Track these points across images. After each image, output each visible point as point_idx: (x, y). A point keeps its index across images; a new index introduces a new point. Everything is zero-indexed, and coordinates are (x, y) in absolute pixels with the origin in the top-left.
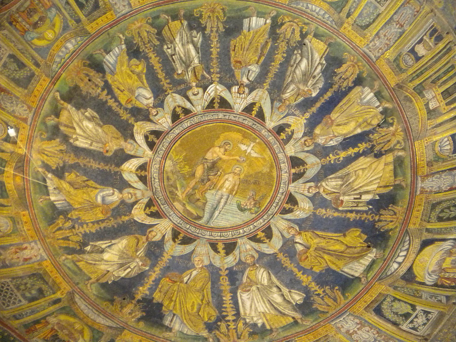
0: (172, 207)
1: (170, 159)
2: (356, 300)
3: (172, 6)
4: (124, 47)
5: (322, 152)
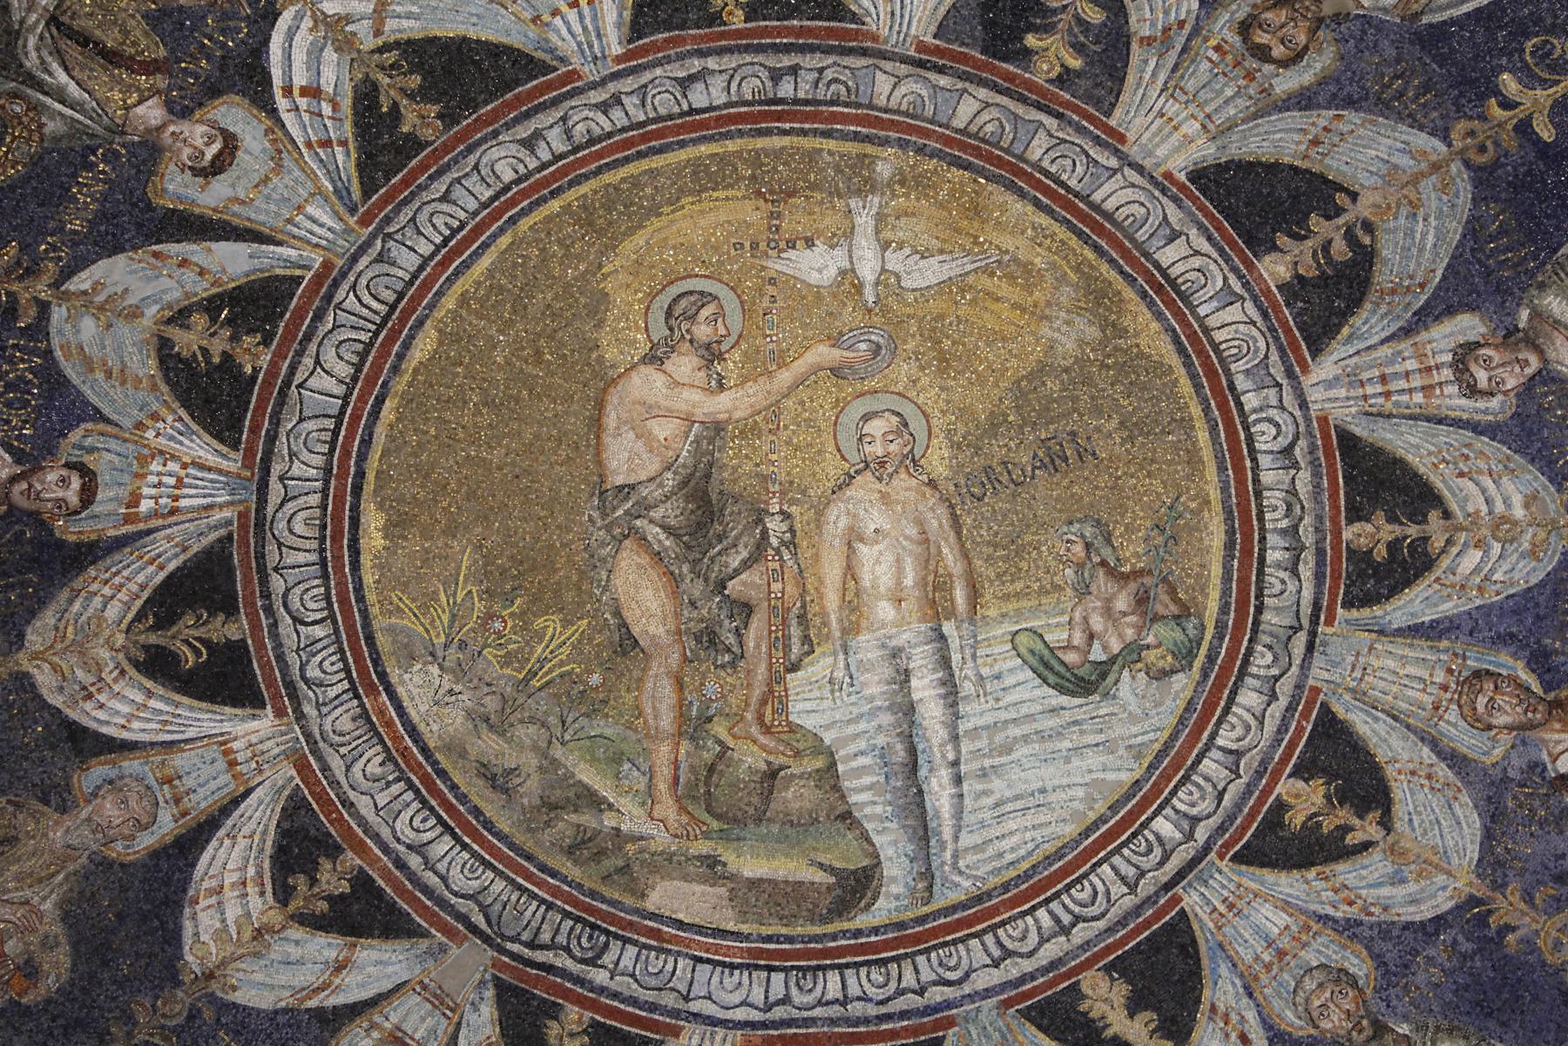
0: (659, 934)
1: (409, 658)
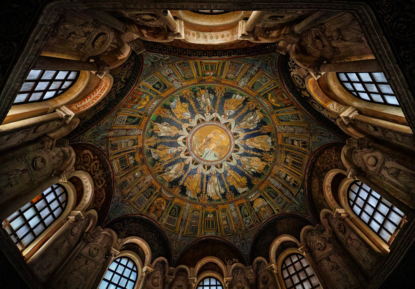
0: (193, 152)
3: (202, 85)
5: (246, 148)
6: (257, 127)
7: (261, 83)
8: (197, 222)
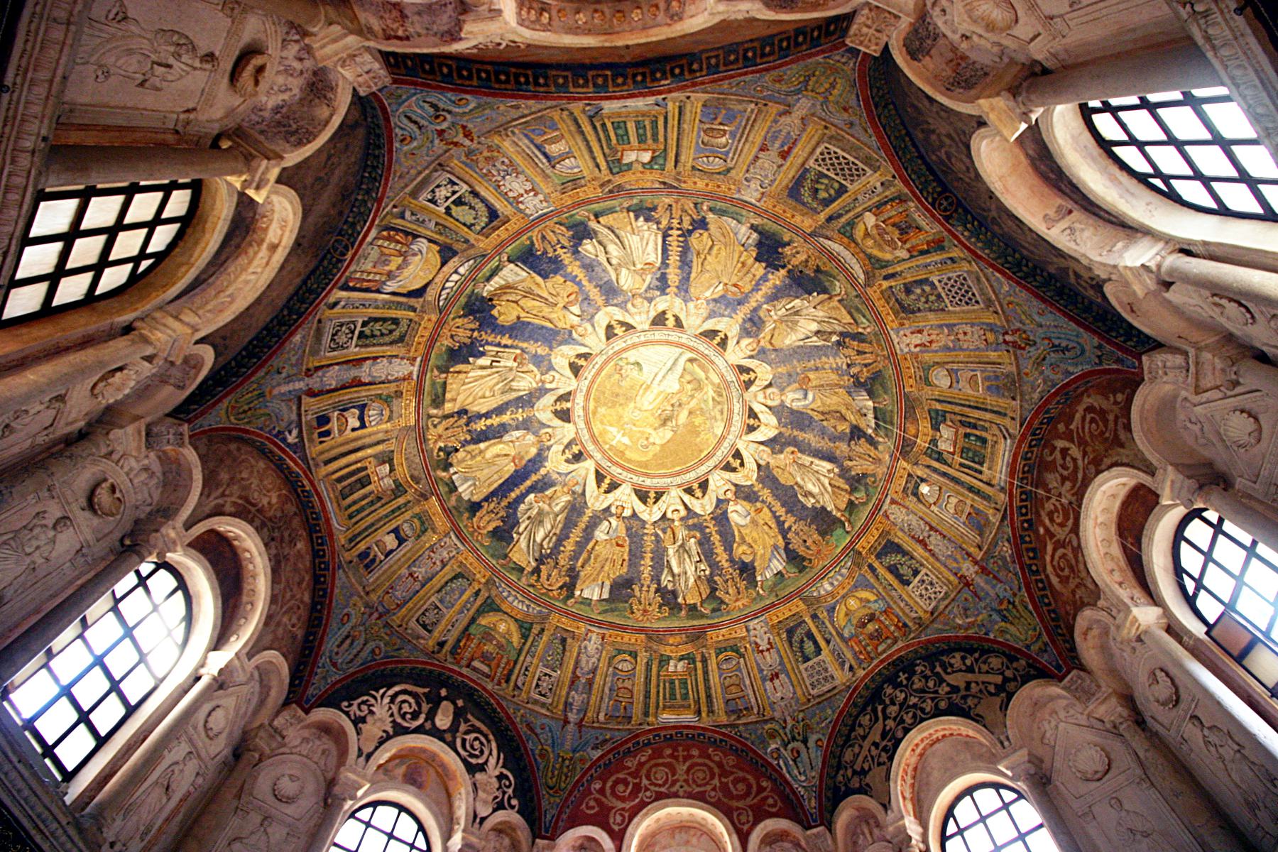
2: (520, 233)
3: (695, 623)
4: (759, 578)
6: (516, 510)
7: (548, 671)
8: (706, 139)
